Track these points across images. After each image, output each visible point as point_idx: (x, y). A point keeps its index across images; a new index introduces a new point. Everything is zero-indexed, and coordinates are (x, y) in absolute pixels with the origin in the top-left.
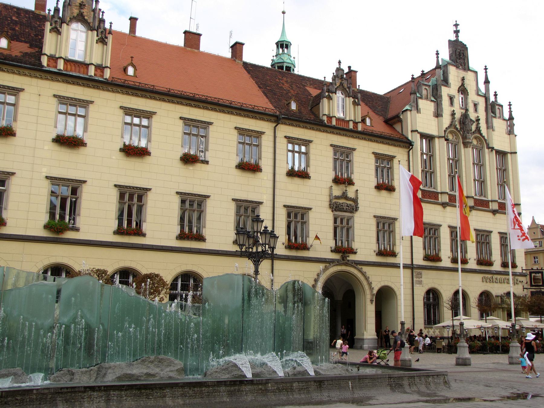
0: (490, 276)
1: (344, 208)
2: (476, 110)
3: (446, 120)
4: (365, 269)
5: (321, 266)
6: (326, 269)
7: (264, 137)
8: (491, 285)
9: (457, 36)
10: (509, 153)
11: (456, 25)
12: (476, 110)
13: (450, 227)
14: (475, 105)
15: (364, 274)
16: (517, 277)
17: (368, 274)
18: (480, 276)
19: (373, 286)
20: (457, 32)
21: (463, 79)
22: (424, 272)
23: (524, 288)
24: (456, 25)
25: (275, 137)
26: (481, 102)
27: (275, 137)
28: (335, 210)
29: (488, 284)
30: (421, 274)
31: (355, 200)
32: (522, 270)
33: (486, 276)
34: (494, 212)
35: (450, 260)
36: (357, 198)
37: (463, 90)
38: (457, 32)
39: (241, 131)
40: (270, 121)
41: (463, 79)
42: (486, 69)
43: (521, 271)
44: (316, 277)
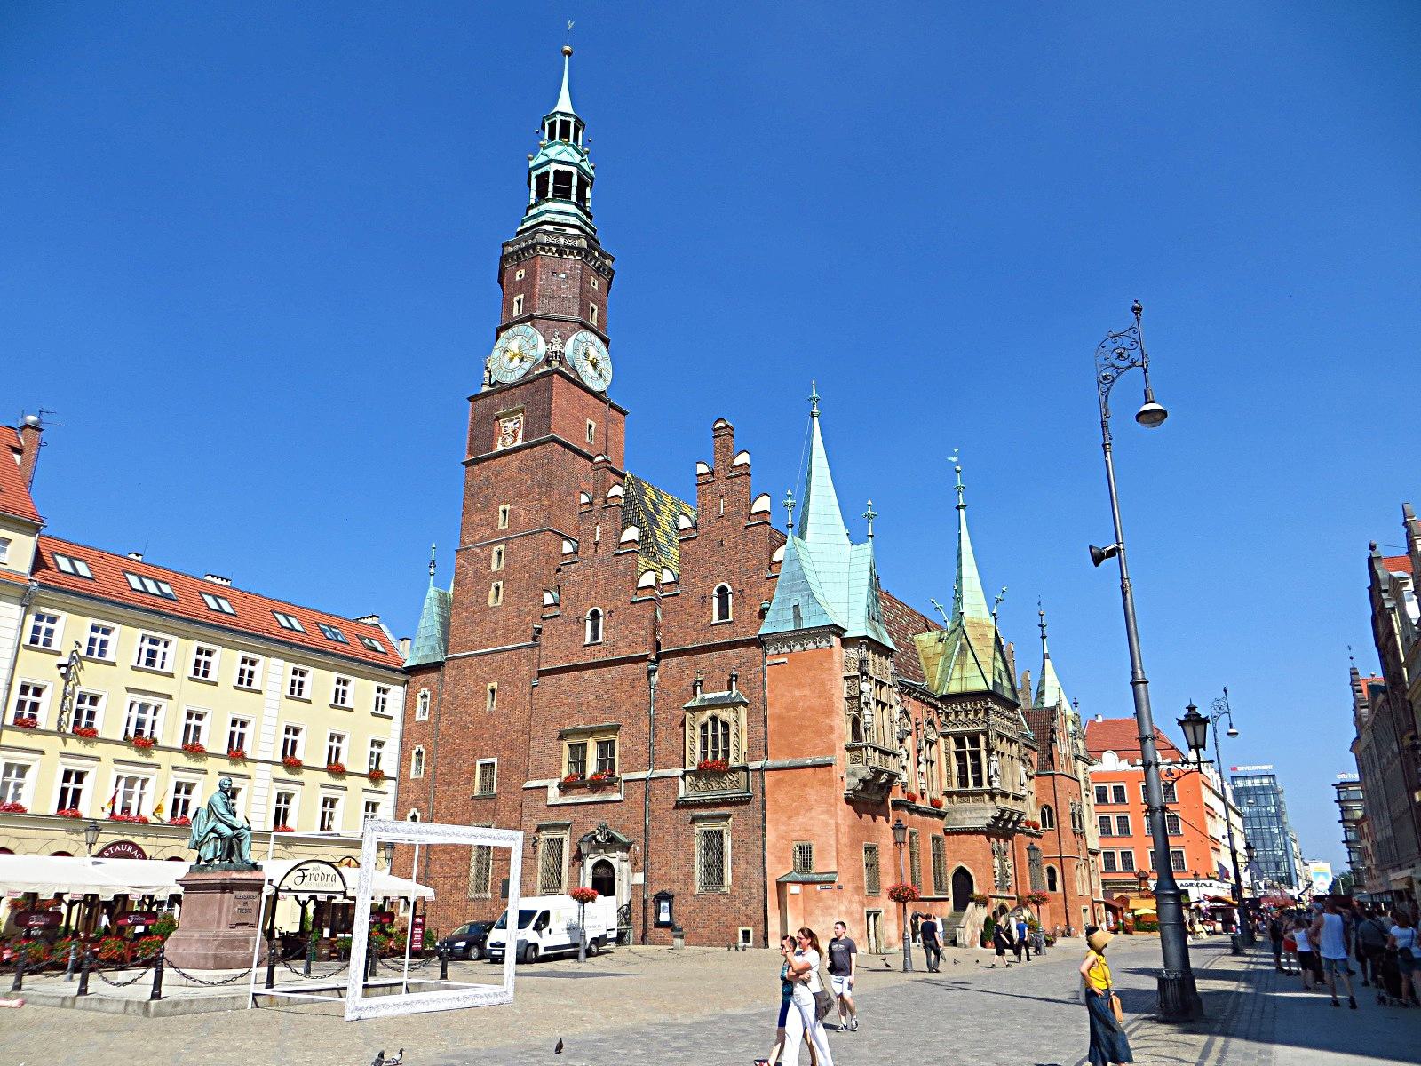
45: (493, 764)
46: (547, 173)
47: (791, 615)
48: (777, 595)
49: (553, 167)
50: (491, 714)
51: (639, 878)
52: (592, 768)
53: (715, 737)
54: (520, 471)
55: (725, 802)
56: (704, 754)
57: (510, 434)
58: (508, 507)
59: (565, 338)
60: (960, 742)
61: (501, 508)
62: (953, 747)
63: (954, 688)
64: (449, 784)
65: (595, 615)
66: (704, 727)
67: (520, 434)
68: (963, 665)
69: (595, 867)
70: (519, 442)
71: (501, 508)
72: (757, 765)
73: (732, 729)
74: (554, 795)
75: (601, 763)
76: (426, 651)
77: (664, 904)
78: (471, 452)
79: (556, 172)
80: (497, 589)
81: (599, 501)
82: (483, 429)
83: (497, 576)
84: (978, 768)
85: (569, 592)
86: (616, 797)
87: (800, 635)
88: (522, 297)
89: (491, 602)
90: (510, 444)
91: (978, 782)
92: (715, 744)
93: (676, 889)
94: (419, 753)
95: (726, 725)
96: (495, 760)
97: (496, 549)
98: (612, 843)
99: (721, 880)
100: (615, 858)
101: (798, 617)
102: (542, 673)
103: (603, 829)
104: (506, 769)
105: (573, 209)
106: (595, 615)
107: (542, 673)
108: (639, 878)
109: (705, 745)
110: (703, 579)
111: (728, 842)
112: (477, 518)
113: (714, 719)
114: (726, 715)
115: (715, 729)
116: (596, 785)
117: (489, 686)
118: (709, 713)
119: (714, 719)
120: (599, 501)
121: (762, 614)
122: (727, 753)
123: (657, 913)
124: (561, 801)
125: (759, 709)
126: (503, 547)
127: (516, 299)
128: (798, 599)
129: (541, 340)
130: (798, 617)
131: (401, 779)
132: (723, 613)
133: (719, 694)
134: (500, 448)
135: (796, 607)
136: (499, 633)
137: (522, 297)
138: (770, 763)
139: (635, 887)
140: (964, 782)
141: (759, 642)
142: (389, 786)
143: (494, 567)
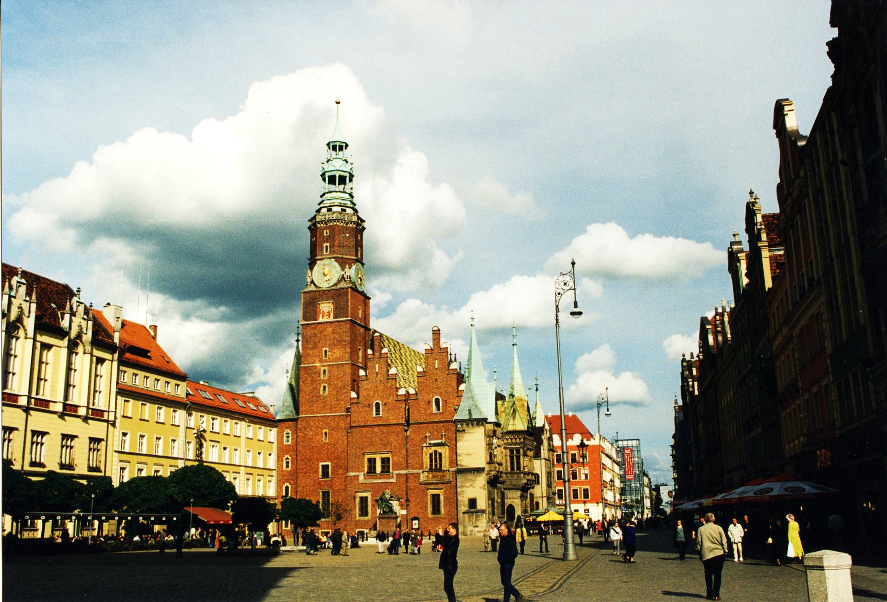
46: (335, 176)
47: (467, 413)
49: (337, 174)
50: (326, 444)
52: (379, 469)
53: (436, 459)
54: (333, 333)
56: (431, 465)
59: (350, 268)
60: (511, 451)
61: (324, 349)
62: (508, 454)
63: (510, 428)
64: (305, 473)
65: (377, 404)
66: (431, 455)
67: (332, 315)
68: (514, 418)
70: (331, 319)
71: (324, 349)
73: (443, 455)
74: (361, 478)
75: (383, 467)
76: (288, 413)
77: (415, 522)
78: (305, 318)
79: (340, 176)
80: (324, 387)
81: (377, 354)
82: (311, 311)
83: (324, 381)
84: (519, 463)
85: (363, 393)
86: (393, 480)
88: (328, 244)
89: (321, 393)
90: (326, 319)
91: (519, 468)
92: (436, 461)
93: (420, 516)
95: (440, 454)
96: (329, 463)
97: (323, 368)
99: (439, 512)
101: (470, 413)
102: (351, 427)
104: (336, 467)
105: (347, 196)
106: (377, 404)
107: (351, 427)
110: (428, 394)
111: (442, 498)
112: (311, 352)
113: (436, 452)
114: (440, 450)
115: (436, 455)
116: (381, 476)
117: (324, 431)
118: (434, 448)
119: (436, 452)
120: (377, 354)
122: (441, 465)
126: (326, 368)
127: (325, 245)
129: (338, 268)
130: (470, 413)
131: (279, 469)
133: (437, 441)
134: (321, 320)
136: (328, 407)
137: (328, 244)
140: (512, 468)
142: (274, 473)
143: (322, 377)
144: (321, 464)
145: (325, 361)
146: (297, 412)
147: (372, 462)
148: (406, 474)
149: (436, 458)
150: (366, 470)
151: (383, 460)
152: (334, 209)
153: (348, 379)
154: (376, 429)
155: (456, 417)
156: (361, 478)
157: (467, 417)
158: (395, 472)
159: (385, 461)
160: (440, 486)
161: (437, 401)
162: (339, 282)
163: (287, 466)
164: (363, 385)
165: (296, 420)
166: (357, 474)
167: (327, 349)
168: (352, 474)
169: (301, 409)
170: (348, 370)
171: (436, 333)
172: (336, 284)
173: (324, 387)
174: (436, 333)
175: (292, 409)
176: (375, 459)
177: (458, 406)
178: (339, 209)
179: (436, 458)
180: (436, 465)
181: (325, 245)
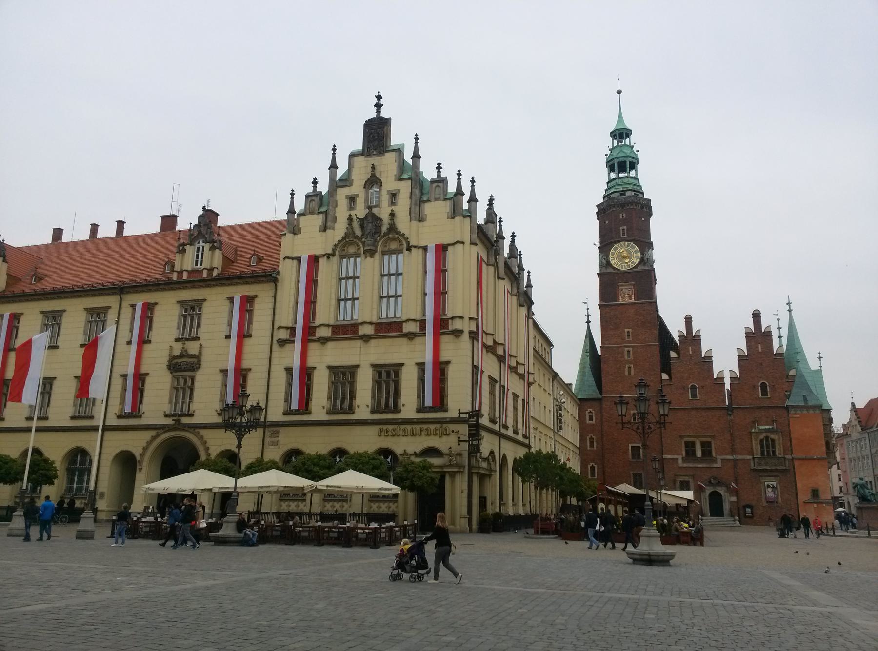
0: (391, 427)
1: (184, 367)
2: (393, 204)
3: (340, 230)
4: (203, 432)
5: (153, 433)
6: (157, 436)
7: (110, 311)
8: (396, 439)
9: (378, 112)
10: (450, 245)
11: (379, 97)
12: (393, 204)
13: (330, 368)
14: (394, 195)
15: (201, 438)
16: (445, 426)
17: (205, 438)
18: (374, 430)
19: (210, 451)
20: (378, 106)
21: (373, 167)
22: (283, 430)
23: (459, 441)
24: (379, 97)
25: (120, 308)
26: (405, 188)
27: (120, 308)
28: (176, 371)
29: (390, 439)
30: (278, 432)
31: (198, 357)
32: (460, 413)
33: (385, 427)
34: (411, 336)
35: (325, 410)
36: (200, 353)
37: (373, 181)
38: (378, 106)
39: (89, 310)
40: (113, 294)
41: (373, 167)
42: (416, 139)
43: (457, 416)
44: (208, 445)
45: (639, 447)
47: (802, 398)
48: (794, 390)
49: (628, 160)
51: (734, 499)
52: (699, 454)
55: (776, 470)
57: (626, 295)
58: (630, 330)
61: (626, 330)
66: (762, 441)
69: (711, 494)
71: (626, 330)
72: (790, 457)
73: (777, 442)
74: (680, 461)
77: (749, 510)
80: (630, 368)
86: (719, 465)
87: (807, 407)
88: (625, 228)
89: (627, 373)
90: (627, 301)
94: (591, 438)
96: (640, 445)
97: (626, 349)
98: (719, 483)
100: (722, 491)
103: (715, 478)
108: (734, 499)
109: (762, 447)
113: (767, 438)
114: (772, 436)
119: (767, 438)
121: (788, 397)
122: (774, 452)
123: (745, 512)
124: (685, 465)
125: (787, 434)
126: (631, 349)
128: (804, 392)
132: (764, 392)
135: (804, 396)
137: (625, 228)
138: (794, 456)
139: (731, 503)
141: (787, 408)
143: (626, 357)
144: (630, 445)
145: (629, 342)
146: (601, 392)
147: (690, 447)
148: (734, 460)
149: (768, 445)
150: (684, 453)
151: (703, 444)
152: (628, 194)
153: (657, 359)
154: (693, 412)
155: (788, 403)
156: (680, 461)
157: (802, 403)
158: (720, 457)
159: (706, 447)
160: (776, 474)
161: (764, 386)
162: (639, 264)
163: (592, 445)
164: (675, 367)
165: (599, 400)
166: (675, 457)
167: (630, 330)
168: (669, 457)
169: (604, 389)
170: (656, 350)
171: (756, 316)
172: (635, 267)
173: (630, 368)
174: (756, 316)
175: (595, 388)
176: (693, 444)
177: (790, 391)
178: (633, 193)
179: (768, 445)
180: (768, 452)
181: (621, 228)
